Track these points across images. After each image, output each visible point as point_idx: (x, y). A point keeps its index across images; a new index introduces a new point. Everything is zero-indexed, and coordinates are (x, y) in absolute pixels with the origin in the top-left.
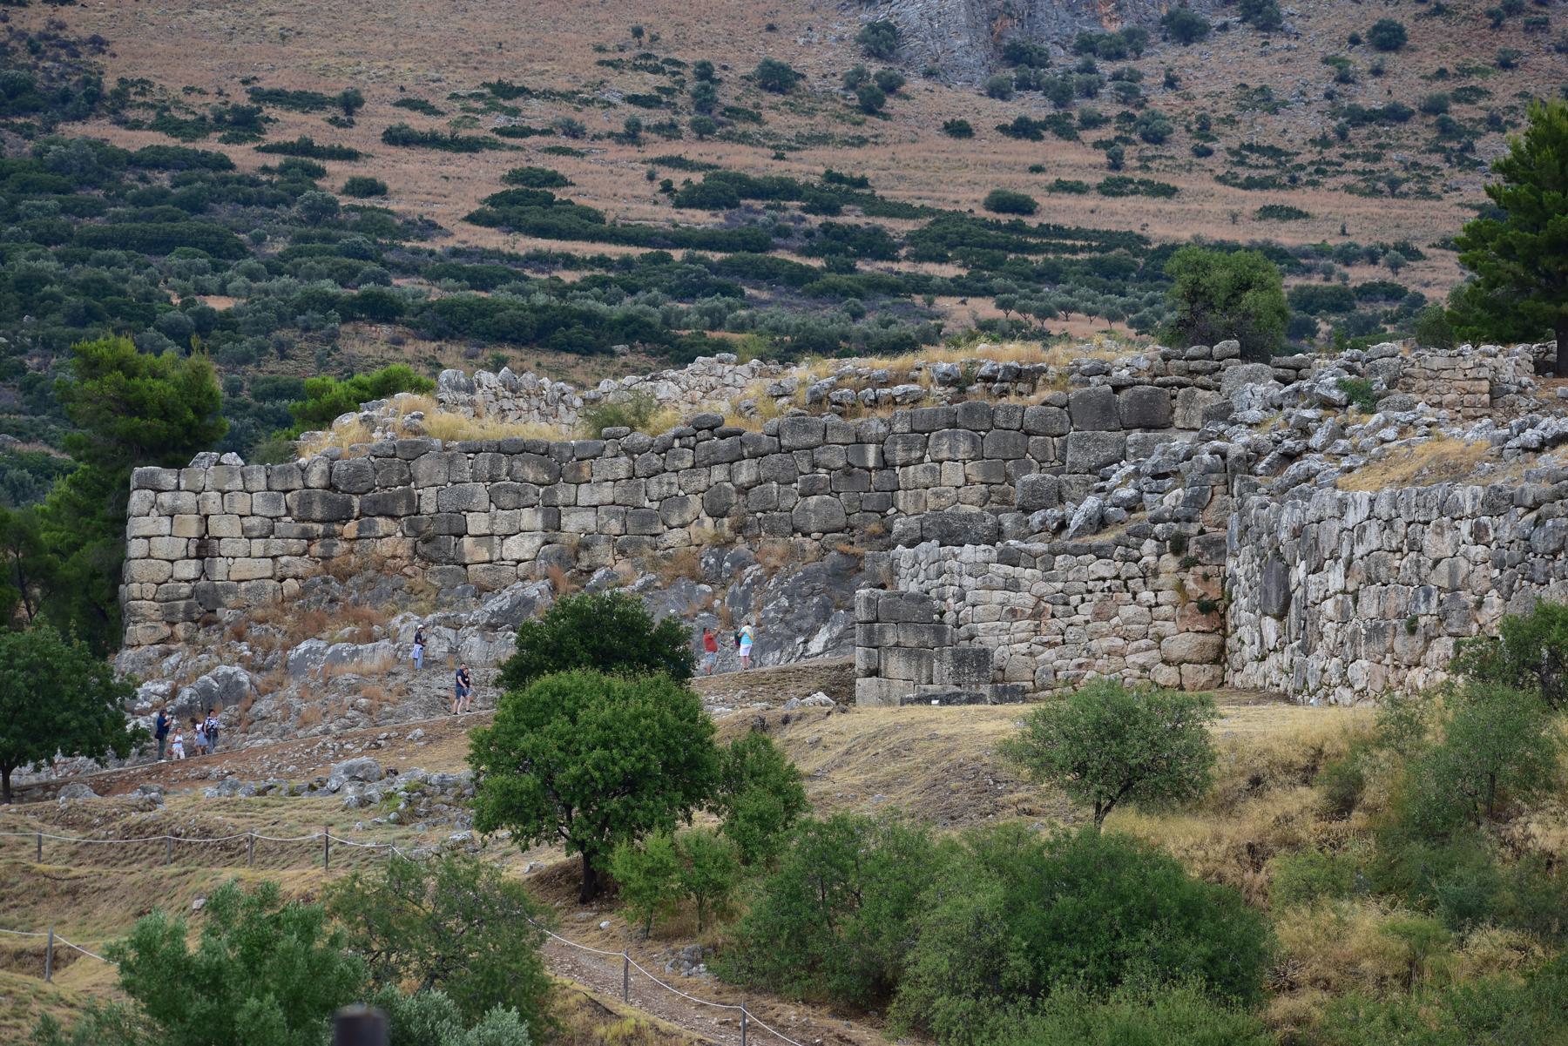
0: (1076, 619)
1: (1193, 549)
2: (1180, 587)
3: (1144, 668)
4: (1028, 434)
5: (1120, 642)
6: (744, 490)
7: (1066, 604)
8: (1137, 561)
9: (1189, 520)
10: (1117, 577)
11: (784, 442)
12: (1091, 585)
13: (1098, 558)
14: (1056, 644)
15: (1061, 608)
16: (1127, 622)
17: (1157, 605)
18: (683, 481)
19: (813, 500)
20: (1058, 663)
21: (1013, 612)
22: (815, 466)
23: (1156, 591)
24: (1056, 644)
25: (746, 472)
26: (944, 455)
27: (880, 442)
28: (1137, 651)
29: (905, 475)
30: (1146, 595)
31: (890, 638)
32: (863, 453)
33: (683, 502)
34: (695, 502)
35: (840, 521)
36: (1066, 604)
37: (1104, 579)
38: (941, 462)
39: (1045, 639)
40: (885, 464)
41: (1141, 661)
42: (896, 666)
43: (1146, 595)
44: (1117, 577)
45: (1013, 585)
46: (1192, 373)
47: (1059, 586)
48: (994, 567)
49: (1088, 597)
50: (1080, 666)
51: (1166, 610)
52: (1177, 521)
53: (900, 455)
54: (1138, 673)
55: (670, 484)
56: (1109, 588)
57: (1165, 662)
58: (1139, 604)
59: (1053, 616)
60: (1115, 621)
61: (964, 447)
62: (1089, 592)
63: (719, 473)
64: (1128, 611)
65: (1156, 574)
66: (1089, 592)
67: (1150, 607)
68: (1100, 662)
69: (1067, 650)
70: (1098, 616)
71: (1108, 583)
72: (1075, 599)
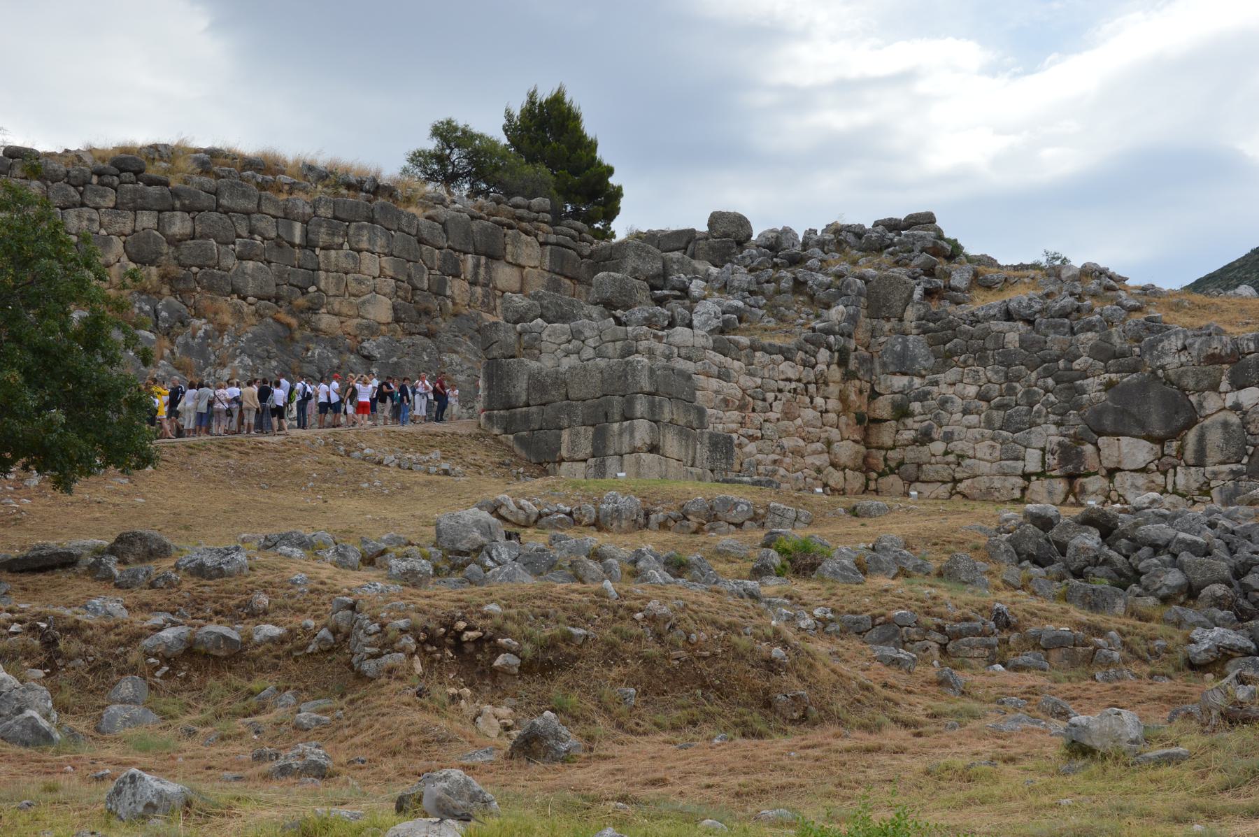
0: (772, 416)
1: (853, 364)
2: (843, 398)
3: (819, 470)
4: (421, 241)
5: (802, 443)
6: (175, 242)
7: (764, 400)
8: (813, 367)
9: (850, 336)
10: (799, 380)
11: (224, 202)
12: (781, 384)
13: (786, 359)
14: (757, 438)
15: (760, 403)
16: (807, 424)
17: (827, 411)
18: (106, 220)
19: (250, 265)
20: (759, 456)
21: (726, 402)
22: (252, 232)
23: (826, 398)
24: (757, 438)
25: (179, 224)
26: (364, 245)
27: (305, 222)
28: (814, 453)
29: (327, 257)
30: (819, 401)
31: (667, 416)
32: (290, 230)
33: (107, 242)
34: (118, 244)
35: (272, 290)
36: (764, 400)
37: (789, 380)
38: (359, 251)
39: (751, 432)
40: (309, 244)
41: (818, 463)
42: (672, 444)
43: (819, 401)
44: (799, 380)
45: (724, 375)
46: (521, 219)
47: (759, 381)
48: (711, 354)
49: (779, 396)
50: (775, 462)
51: (832, 417)
52: (842, 335)
53: (323, 238)
54: (814, 474)
55: (91, 220)
56: (795, 390)
57: (833, 465)
58: (814, 408)
59: (754, 410)
60: (799, 421)
61: (380, 242)
62: (780, 391)
63: (147, 220)
64: (809, 414)
65: (826, 384)
66: (780, 391)
67: (821, 412)
68: (787, 460)
69: (765, 445)
70: (788, 415)
71: (794, 385)
72: (770, 396)
